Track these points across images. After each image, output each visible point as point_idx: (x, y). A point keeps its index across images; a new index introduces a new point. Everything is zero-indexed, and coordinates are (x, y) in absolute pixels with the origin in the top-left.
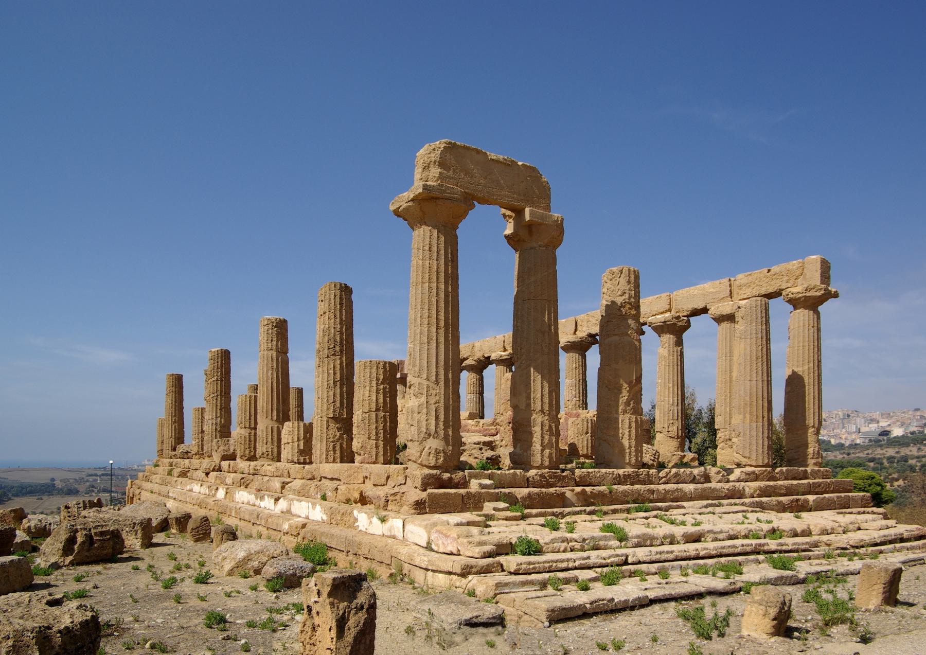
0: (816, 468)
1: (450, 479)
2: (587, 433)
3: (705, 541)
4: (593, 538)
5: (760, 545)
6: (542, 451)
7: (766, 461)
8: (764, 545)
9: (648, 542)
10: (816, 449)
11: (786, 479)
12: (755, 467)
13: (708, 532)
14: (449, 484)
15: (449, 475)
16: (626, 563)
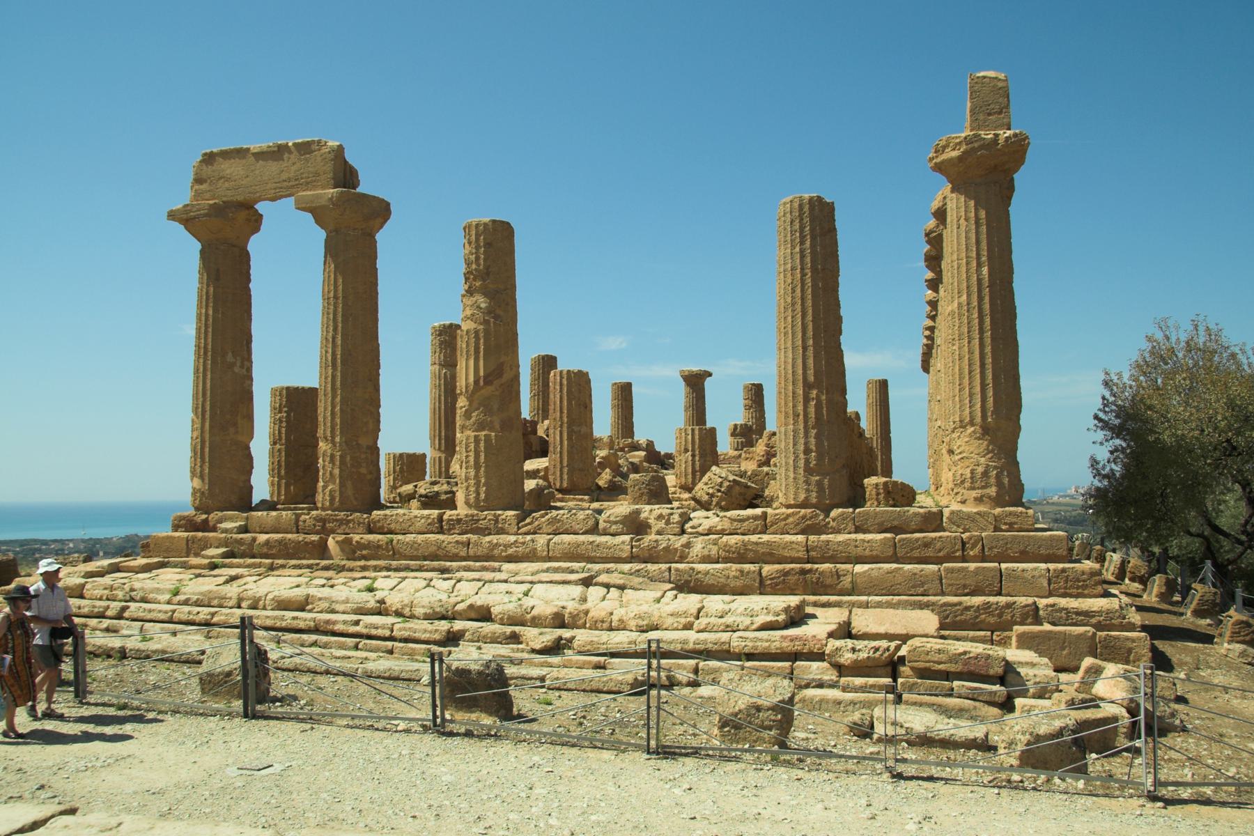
0: (982, 508)
1: (206, 521)
2: (686, 451)
3: (310, 611)
4: (142, 589)
5: (328, 622)
6: (325, 487)
7: (802, 496)
8: (335, 623)
9: (215, 602)
10: (980, 469)
11: (858, 530)
12: (788, 506)
13: (320, 599)
14: (205, 527)
15: (204, 516)
16: (101, 616)
